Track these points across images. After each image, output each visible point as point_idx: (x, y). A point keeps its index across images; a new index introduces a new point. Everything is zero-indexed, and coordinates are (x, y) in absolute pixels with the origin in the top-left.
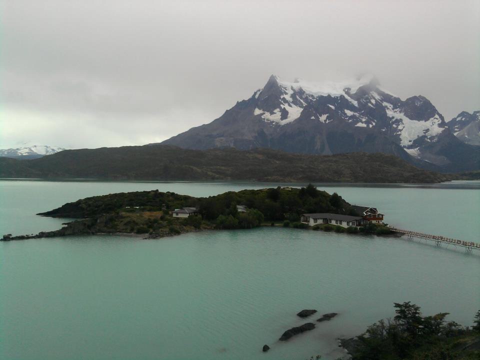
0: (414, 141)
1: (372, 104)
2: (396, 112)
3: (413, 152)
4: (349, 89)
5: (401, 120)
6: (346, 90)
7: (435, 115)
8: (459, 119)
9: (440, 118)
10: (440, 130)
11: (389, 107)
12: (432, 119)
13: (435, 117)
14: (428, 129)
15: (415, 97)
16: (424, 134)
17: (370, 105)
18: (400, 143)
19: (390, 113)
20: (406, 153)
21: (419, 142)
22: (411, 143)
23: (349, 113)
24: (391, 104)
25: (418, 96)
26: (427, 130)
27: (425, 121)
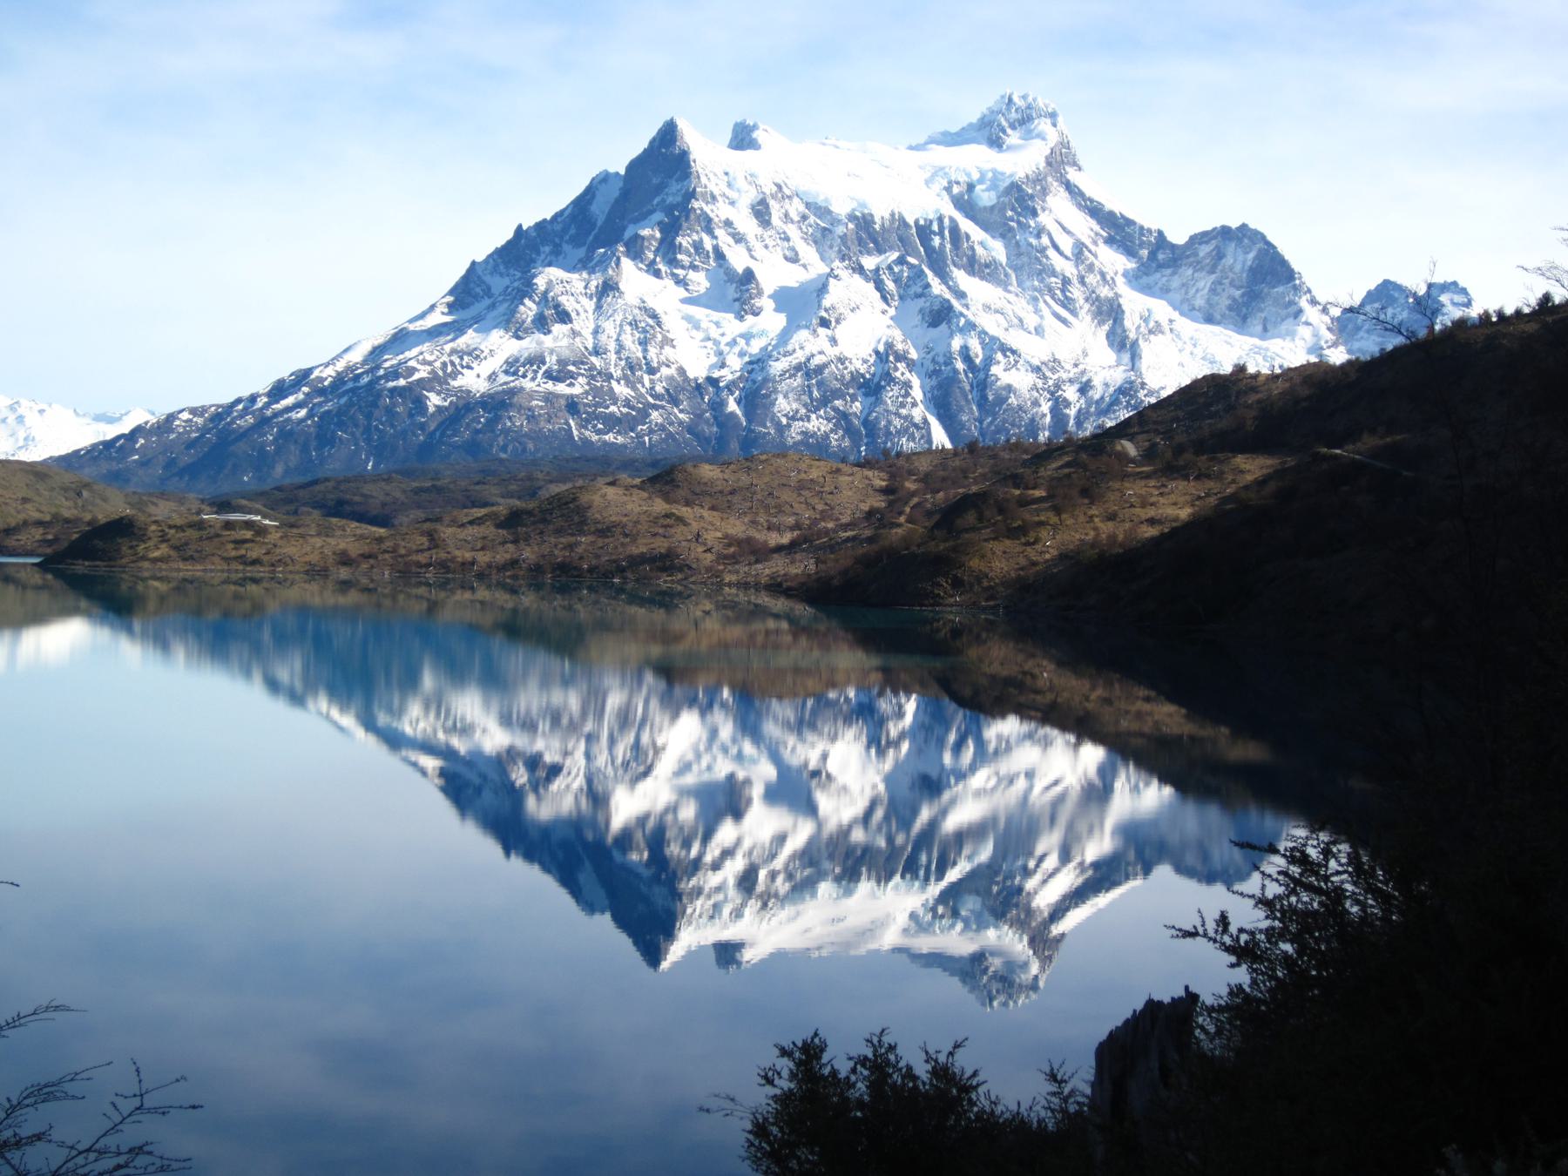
6: (956, 190)
15: (1225, 232)
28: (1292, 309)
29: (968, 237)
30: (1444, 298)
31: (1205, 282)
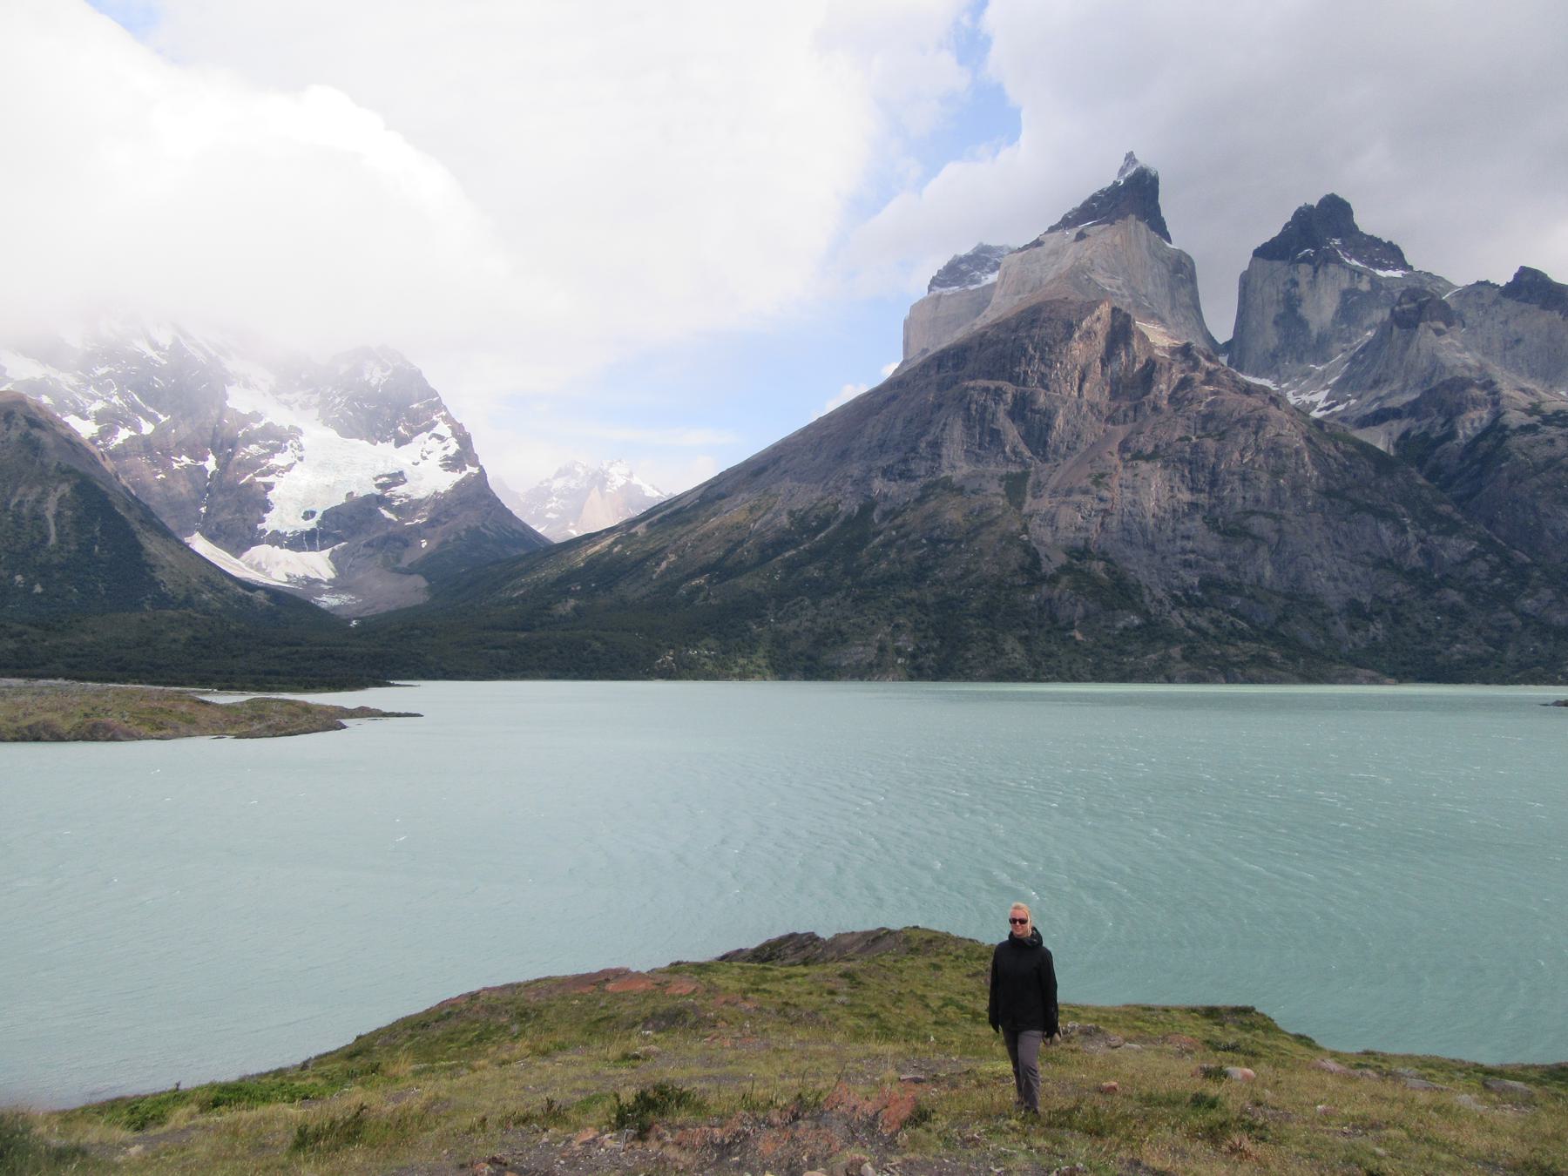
0: (326, 515)
5: (296, 432)
7: (434, 424)
8: (558, 484)
9: (454, 435)
10: (445, 481)
12: (425, 435)
13: (436, 430)
14: (401, 473)
16: (378, 492)
18: (262, 520)
21: (350, 525)
26: (398, 478)
27: (398, 445)
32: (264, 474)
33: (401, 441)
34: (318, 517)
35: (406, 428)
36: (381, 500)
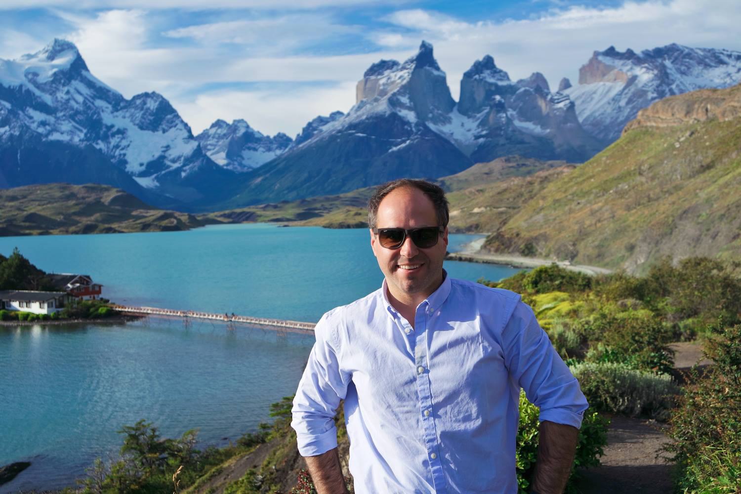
1: (77, 102)
2: (117, 116)
3: (145, 182)
4: (36, 74)
6: (30, 76)
11: (104, 108)
12: (173, 129)
13: (178, 127)
15: (146, 95)
16: (163, 154)
17: (72, 103)
18: (126, 168)
19: (108, 118)
20: (136, 183)
21: (155, 167)
22: (143, 168)
23: (38, 116)
24: (110, 103)
25: (150, 91)
26: (168, 147)
28: (174, 124)
29: (34, 94)
30: (239, 125)
31: (139, 114)
32: (123, 149)
33: (164, 131)
34: (145, 164)
35: (166, 126)
36: (162, 157)
